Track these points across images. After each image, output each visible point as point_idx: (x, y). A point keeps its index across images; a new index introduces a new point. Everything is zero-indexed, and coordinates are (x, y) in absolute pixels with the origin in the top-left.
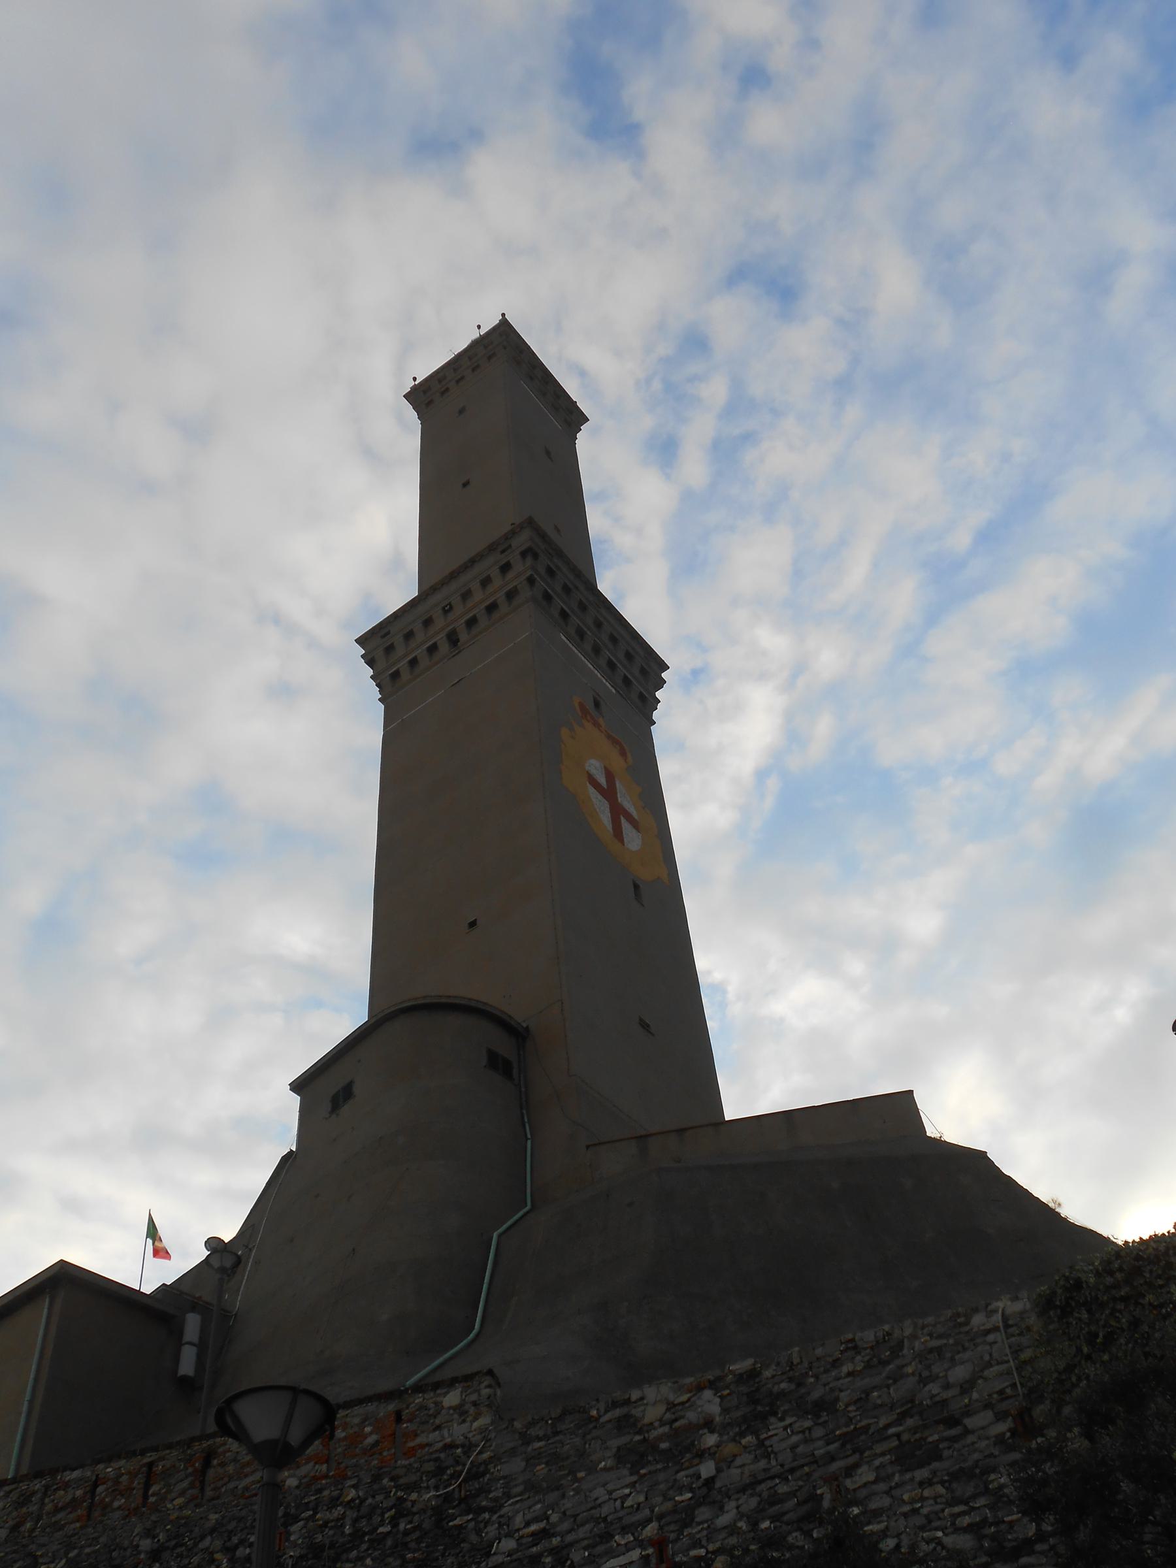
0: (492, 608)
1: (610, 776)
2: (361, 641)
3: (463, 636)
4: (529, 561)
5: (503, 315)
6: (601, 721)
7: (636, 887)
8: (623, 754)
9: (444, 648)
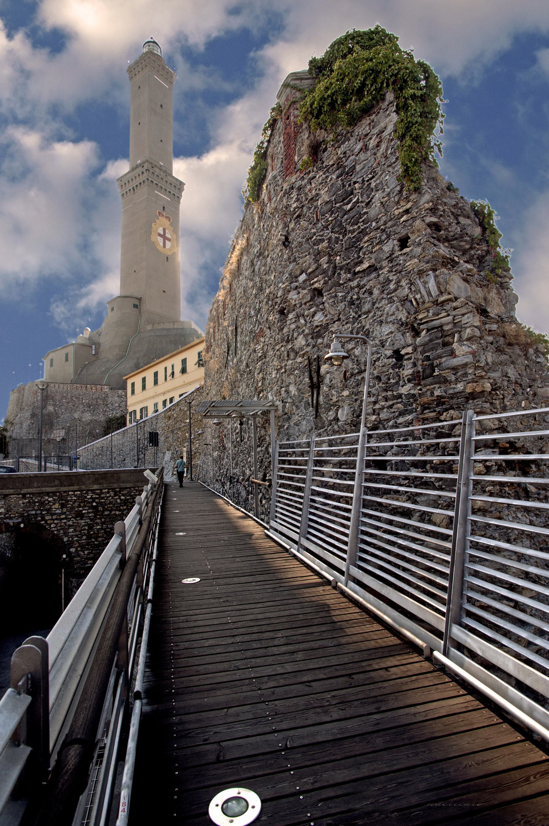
0: (140, 183)
1: (164, 230)
8: (170, 220)
9: (132, 191)
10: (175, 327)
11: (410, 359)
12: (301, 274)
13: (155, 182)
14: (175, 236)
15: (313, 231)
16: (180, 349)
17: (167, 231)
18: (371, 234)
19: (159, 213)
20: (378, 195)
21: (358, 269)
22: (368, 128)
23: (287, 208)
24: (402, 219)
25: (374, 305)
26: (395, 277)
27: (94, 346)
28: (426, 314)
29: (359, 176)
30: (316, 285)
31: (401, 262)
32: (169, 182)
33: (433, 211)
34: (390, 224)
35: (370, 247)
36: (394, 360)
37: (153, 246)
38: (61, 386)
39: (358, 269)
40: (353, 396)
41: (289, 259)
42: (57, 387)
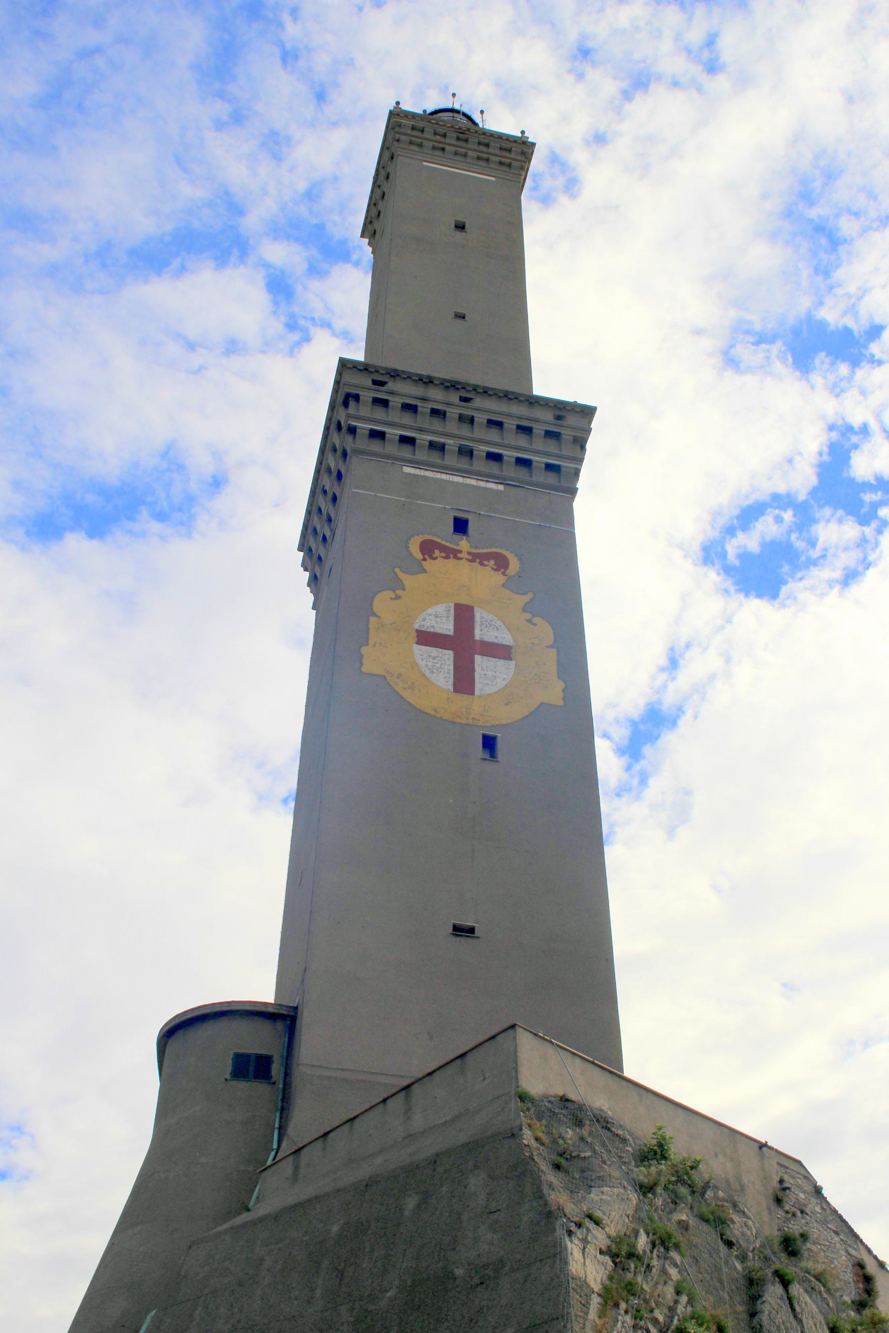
1: (464, 615)
4: (352, 403)
5: (398, 103)
7: (489, 743)
13: (393, 433)
14: (544, 631)
17: (479, 615)
19: (428, 548)
32: (481, 418)
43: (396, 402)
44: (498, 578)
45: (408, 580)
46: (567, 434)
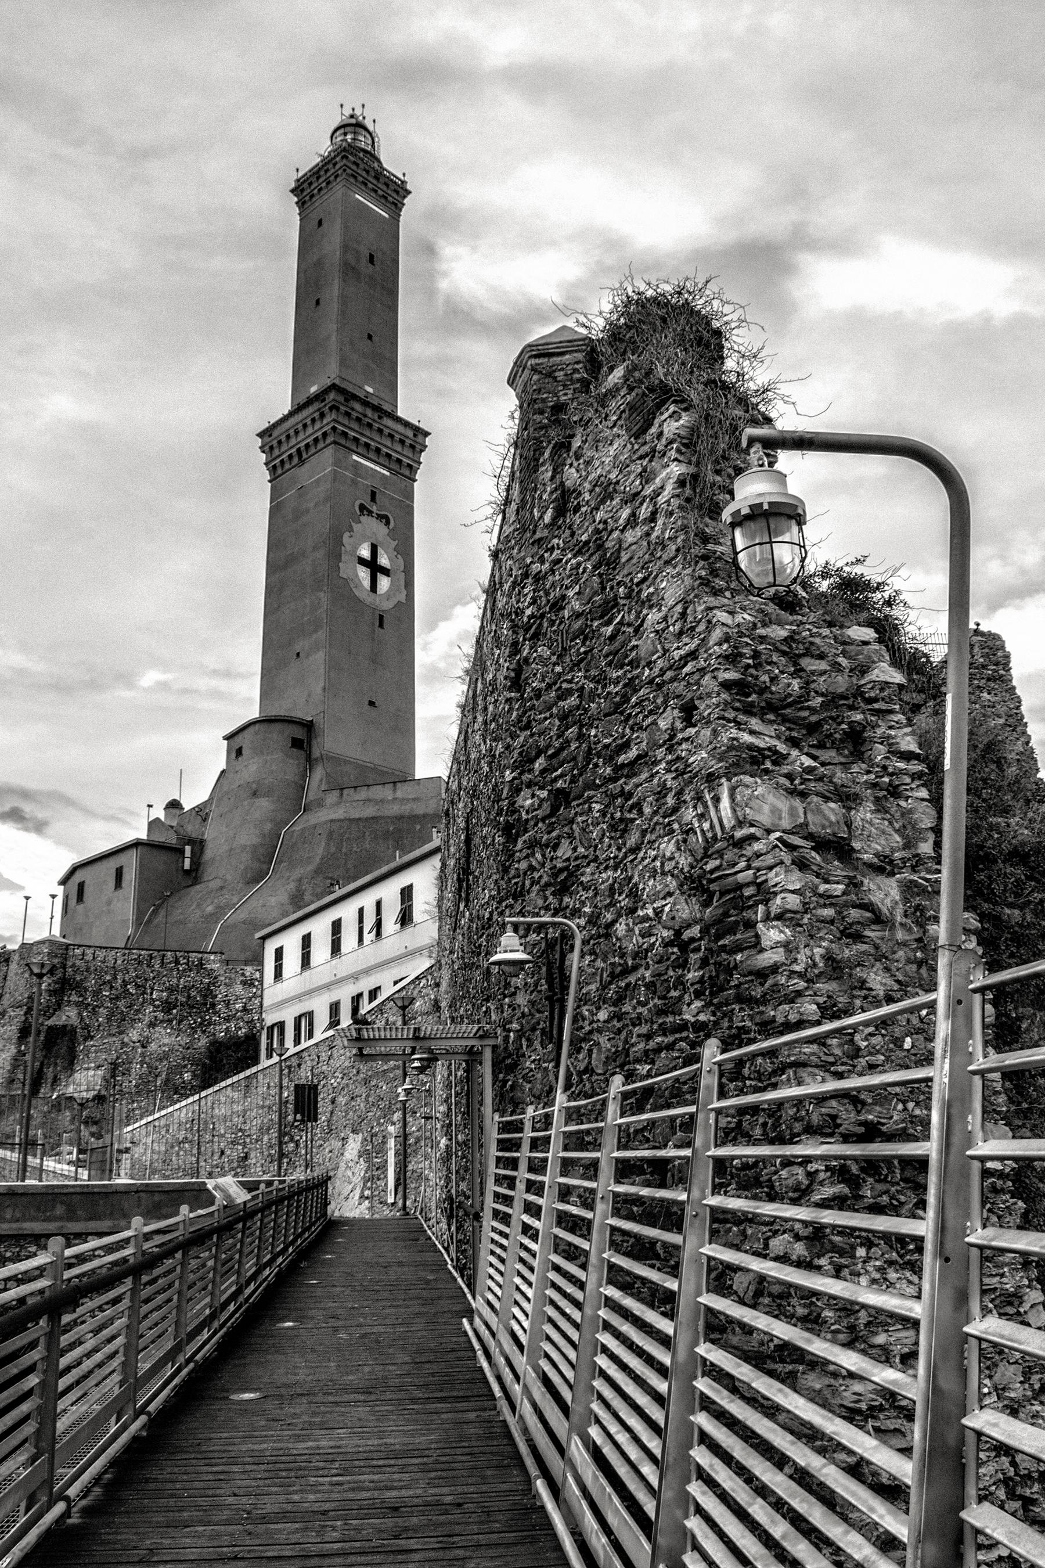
2: (261, 435)
3: (305, 456)
6: (374, 509)
7: (381, 617)
8: (388, 523)
9: (296, 460)
10: (399, 794)
11: (698, 950)
12: (537, 757)
14: (401, 561)
15: (558, 669)
16: (399, 861)
17: (380, 550)
18: (641, 693)
19: (362, 507)
20: (653, 617)
21: (622, 759)
22: (638, 482)
23: (517, 615)
24: (687, 669)
25: (644, 836)
26: (675, 784)
27: (188, 848)
28: (717, 862)
29: (625, 572)
30: (560, 784)
31: (683, 754)
33: (732, 659)
34: (669, 674)
35: (641, 716)
36: (675, 950)
37: (343, 591)
38: (101, 954)
39: (622, 759)
40: (615, 1022)
41: (520, 721)
42: (89, 957)
43: (354, 414)
44: (385, 530)
45: (355, 526)
46: (418, 447)
